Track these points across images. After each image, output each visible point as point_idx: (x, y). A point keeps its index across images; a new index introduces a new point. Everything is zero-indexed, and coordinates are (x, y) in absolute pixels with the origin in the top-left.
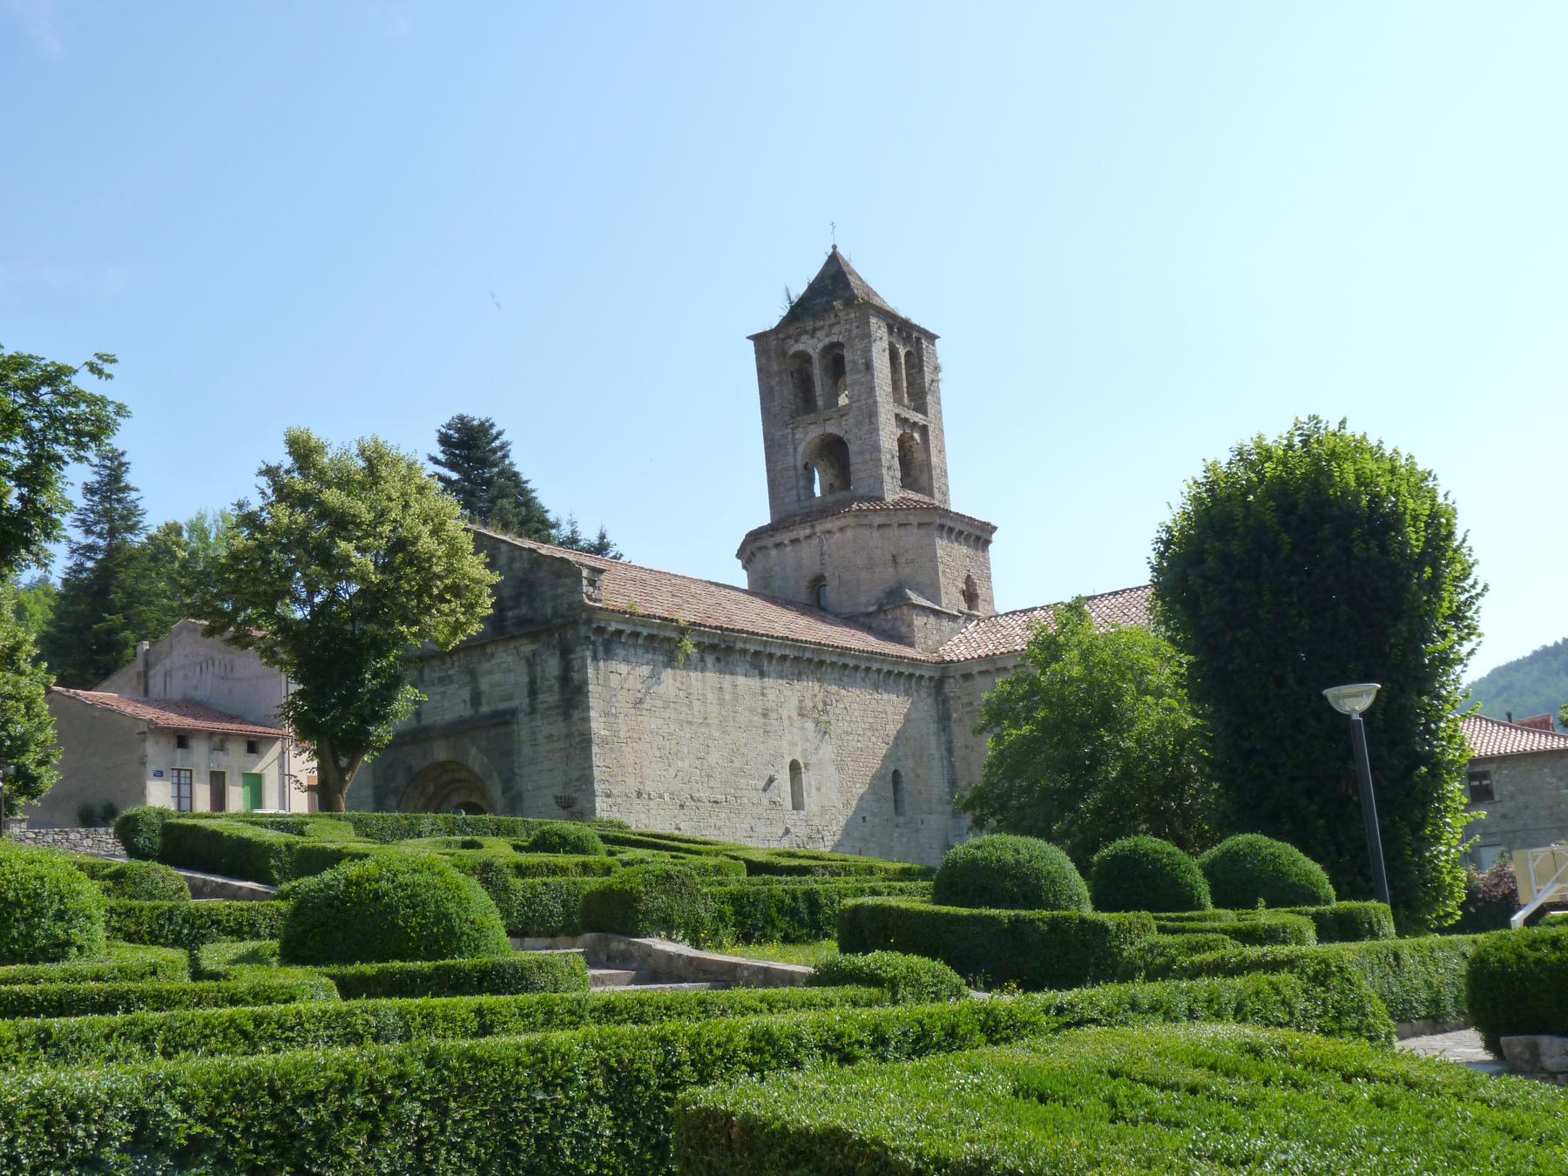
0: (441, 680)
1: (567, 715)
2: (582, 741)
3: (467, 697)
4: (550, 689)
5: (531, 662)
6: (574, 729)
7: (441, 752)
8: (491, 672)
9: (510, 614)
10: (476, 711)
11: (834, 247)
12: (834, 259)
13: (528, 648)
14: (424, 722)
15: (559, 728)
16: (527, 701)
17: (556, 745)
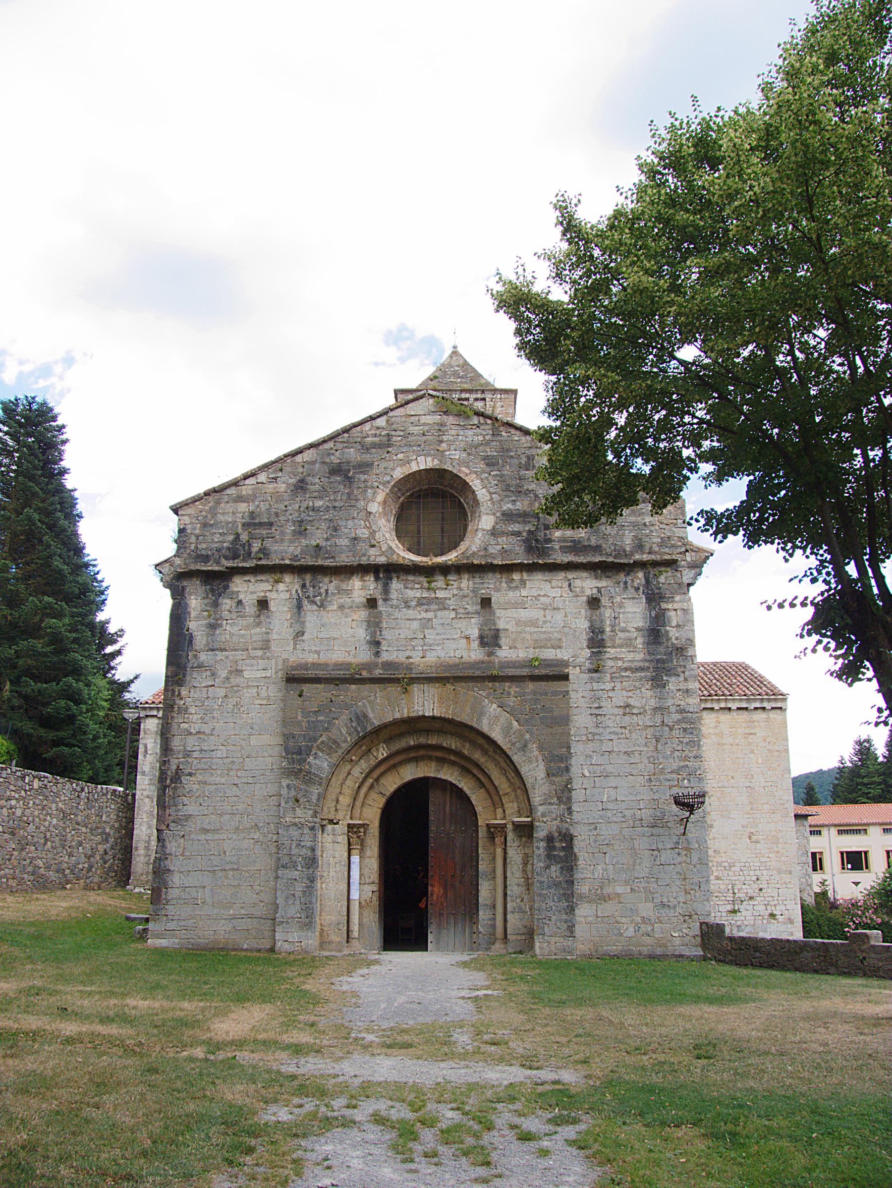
0: (421, 602)
1: (658, 682)
2: (683, 720)
3: (475, 633)
4: (628, 643)
5: (594, 603)
6: (670, 702)
7: (426, 703)
8: (520, 605)
9: (558, 534)
10: (490, 654)
11: (455, 347)
12: (455, 353)
13: (588, 584)
14: (385, 657)
15: (645, 697)
16: (587, 653)
17: (640, 720)
